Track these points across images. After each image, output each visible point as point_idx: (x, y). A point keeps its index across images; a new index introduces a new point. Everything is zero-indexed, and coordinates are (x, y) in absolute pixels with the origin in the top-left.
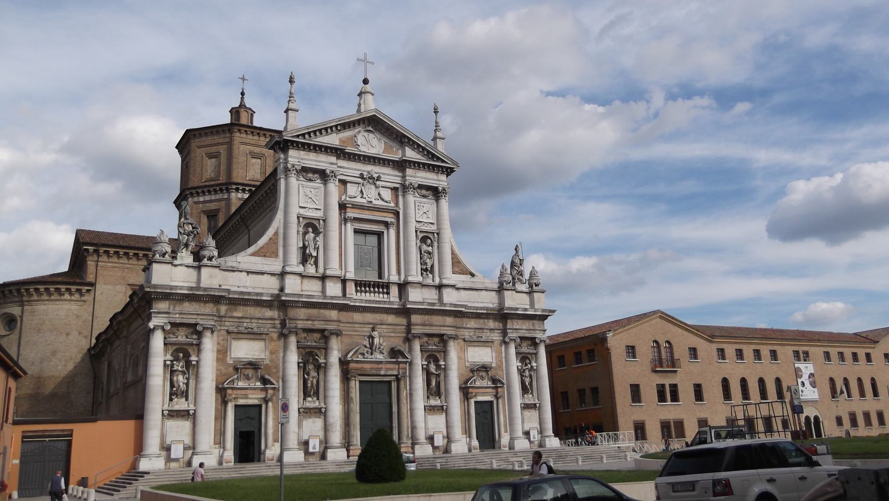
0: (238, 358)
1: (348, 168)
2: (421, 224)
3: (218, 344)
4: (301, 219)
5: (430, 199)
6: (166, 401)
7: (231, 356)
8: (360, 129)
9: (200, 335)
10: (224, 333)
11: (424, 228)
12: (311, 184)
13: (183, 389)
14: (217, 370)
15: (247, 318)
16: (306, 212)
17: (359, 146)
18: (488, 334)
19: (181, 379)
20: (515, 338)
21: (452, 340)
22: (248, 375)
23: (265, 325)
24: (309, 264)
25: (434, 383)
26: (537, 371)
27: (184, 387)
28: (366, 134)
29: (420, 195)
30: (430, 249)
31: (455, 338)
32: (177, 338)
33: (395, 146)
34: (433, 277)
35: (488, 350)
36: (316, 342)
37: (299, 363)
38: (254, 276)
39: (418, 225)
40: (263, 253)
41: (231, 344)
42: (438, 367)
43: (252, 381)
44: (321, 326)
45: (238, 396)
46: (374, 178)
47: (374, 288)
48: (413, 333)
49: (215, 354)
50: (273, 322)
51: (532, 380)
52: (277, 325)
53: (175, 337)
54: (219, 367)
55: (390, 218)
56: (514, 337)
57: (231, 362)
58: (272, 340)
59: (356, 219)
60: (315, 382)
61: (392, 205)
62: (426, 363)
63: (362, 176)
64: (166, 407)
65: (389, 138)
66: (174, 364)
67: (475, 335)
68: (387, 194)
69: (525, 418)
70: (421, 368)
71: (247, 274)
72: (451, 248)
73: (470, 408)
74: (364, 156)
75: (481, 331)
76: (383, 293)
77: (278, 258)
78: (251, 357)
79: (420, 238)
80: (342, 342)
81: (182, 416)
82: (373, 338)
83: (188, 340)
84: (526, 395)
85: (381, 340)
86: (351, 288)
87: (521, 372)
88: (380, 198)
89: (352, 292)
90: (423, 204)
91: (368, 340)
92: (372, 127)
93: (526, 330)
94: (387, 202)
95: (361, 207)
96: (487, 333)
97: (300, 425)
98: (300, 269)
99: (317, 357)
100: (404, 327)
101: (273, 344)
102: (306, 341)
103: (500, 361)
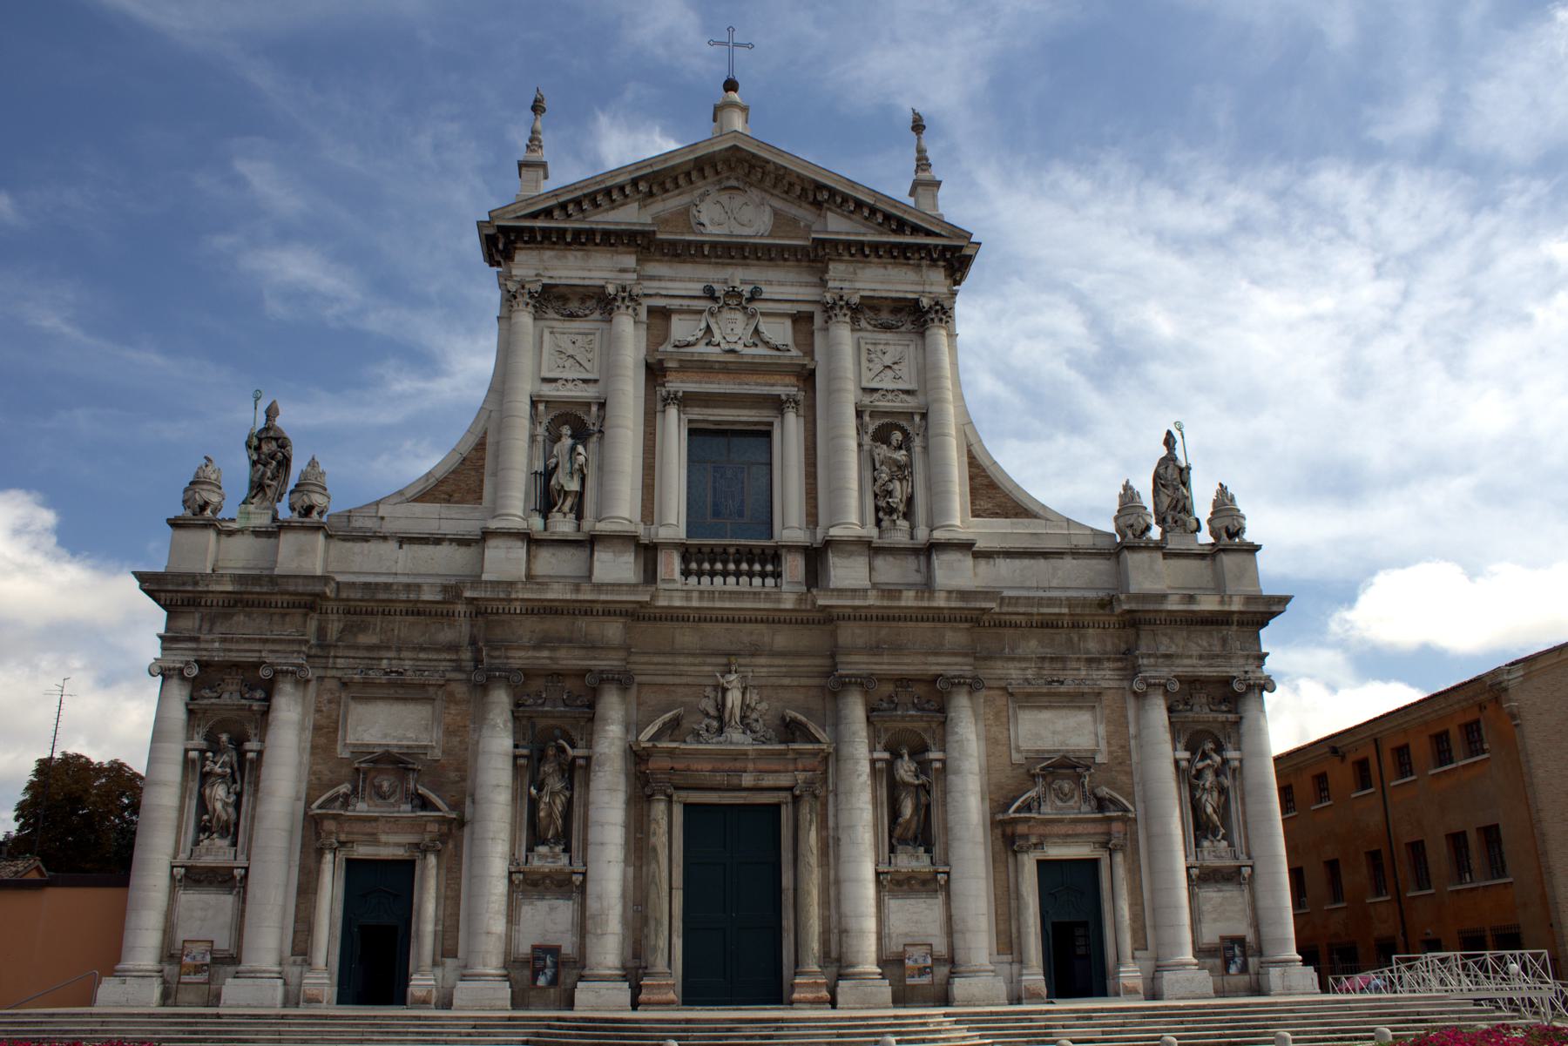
0: (362, 745)
1: (672, 280)
2: (876, 396)
3: (318, 711)
4: (541, 407)
5: (901, 332)
6: (185, 846)
7: (345, 740)
8: (708, 188)
9: (269, 690)
10: (331, 684)
11: (884, 404)
12: (577, 325)
13: (224, 817)
14: (309, 774)
15: (388, 648)
16: (558, 390)
20: (1162, 681)
21: (965, 689)
22: (381, 786)
23: (432, 664)
24: (560, 510)
25: (907, 809)
27: (226, 811)
28: (724, 198)
29: (875, 326)
30: (901, 456)
31: (974, 686)
32: (219, 697)
33: (804, 213)
34: (912, 527)
35: (1085, 717)
36: (566, 705)
37: (515, 757)
38: (416, 547)
39: (867, 400)
40: (445, 493)
42: (923, 767)
43: (392, 800)
44: (574, 662)
45: (355, 837)
46: (740, 295)
47: (738, 563)
48: (841, 676)
49: (308, 735)
50: (454, 657)
51: (1227, 801)
52: (464, 664)
53: (215, 695)
54: (315, 768)
55: (784, 388)
56: (1159, 678)
57: (346, 755)
58: (451, 699)
59: (685, 401)
61: (794, 352)
62: (886, 755)
63: (710, 294)
64: (183, 857)
66: (207, 759)
67: (1040, 676)
68: (779, 332)
70: (865, 768)
71: (397, 545)
72: (969, 452)
73: (1020, 879)
75: (1059, 665)
76: (763, 575)
77: (481, 504)
78: (395, 742)
79: (871, 429)
80: (639, 704)
81: (220, 882)
82: (725, 690)
83: (243, 702)
85: (753, 698)
86: (671, 565)
87: (1189, 778)
88: (762, 340)
89: (673, 575)
90: (881, 347)
91: (712, 695)
92: (737, 179)
94: (778, 349)
95: (705, 367)
96: (1079, 669)
97: (512, 917)
99: (561, 741)
100: (818, 661)
101: (453, 710)
102: (540, 701)
103: (1123, 747)
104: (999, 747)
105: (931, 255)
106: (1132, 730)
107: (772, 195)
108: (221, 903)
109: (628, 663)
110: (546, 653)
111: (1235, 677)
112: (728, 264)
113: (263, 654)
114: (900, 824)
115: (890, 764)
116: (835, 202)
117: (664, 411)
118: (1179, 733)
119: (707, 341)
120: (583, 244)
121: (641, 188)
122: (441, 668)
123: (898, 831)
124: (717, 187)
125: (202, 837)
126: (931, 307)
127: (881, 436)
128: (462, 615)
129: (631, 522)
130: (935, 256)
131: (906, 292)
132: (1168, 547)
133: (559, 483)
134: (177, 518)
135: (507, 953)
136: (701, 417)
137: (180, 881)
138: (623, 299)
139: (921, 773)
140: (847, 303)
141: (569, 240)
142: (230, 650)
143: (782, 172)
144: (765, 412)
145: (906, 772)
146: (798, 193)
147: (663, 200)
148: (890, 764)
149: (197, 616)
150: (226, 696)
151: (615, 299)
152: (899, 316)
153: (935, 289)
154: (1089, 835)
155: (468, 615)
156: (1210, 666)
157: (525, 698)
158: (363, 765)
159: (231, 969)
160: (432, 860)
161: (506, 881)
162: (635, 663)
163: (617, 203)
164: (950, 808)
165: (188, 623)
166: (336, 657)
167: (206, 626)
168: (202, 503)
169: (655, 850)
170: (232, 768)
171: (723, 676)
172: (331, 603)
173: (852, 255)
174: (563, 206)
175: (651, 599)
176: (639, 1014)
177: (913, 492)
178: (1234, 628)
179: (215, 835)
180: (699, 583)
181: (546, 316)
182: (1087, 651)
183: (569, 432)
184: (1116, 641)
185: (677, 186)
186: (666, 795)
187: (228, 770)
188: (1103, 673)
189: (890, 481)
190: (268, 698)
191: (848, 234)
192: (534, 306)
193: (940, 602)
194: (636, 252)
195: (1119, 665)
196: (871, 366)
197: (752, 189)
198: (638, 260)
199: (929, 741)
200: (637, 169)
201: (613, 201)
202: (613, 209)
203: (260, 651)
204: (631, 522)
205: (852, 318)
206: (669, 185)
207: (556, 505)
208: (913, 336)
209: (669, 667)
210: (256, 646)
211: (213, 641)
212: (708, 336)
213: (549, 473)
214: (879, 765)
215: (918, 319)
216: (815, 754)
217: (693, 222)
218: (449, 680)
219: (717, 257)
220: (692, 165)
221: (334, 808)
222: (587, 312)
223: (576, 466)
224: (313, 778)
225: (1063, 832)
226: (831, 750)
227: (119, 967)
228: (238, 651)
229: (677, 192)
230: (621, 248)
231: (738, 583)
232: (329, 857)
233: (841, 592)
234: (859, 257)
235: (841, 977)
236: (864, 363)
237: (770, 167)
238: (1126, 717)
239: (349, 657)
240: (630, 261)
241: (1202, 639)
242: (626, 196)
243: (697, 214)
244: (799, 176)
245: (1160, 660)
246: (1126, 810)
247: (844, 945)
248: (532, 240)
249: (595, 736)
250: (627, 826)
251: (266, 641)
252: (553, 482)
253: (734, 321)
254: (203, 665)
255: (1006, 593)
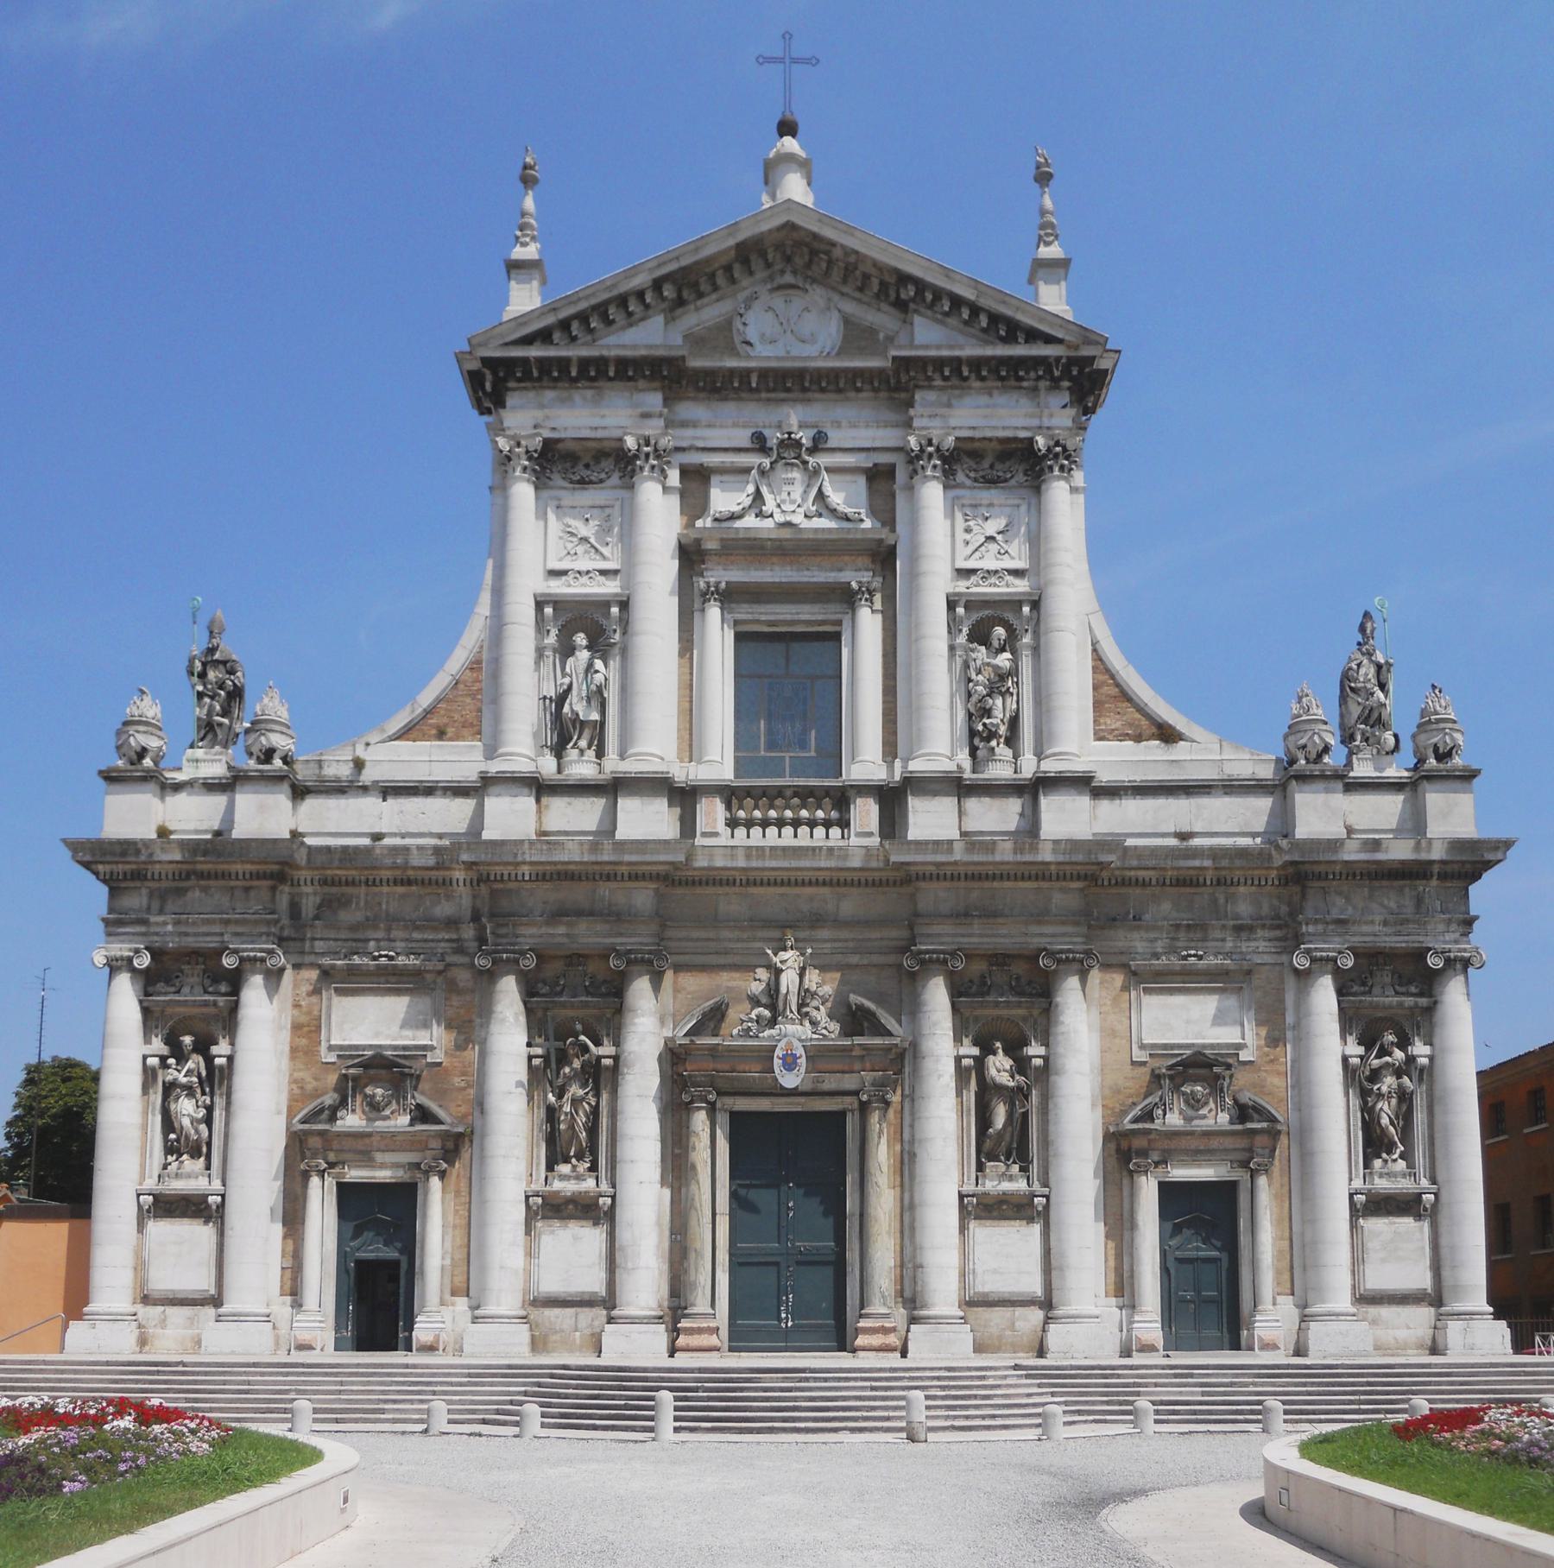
2: (974, 579)
3: (297, 1006)
5: (1010, 488)
6: (151, 1170)
9: (235, 982)
14: (290, 1083)
16: (569, 586)
17: (749, 343)
18: (1229, 945)
19: (187, 1109)
26: (1427, 1075)
27: (197, 1131)
28: (778, 301)
29: (976, 480)
33: (882, 319)
34: (1016, 756)
36: (588, 994)
37: (530, 1058)
41: (329, 1007)
43: (387, 1112)
46: (798, 444)
48: (920, 952)
49: (286, 1036)
50: (454, 936)
52: (466, 944)
53: (173, 989)
54: (296, 1075)
57: (332, 1058)
58: (453, 988)
60: (581, 1119)
61: (868, 524)
62: (976, 1051)
64: (150, 1183)
65: (859, 301)
69: (1372, 1245)
72: (1095, 650)
74: (764, 374)
75: (1199, 935)
76: (827, 824)
80: (676, 991)
83: (207, 998)
84: (1377, 1163)
86: (712, 813)
87: (1360, 1081)
92: (795, 272)
93: (1385, 923)
94: (848, 519)
96: (1223, 940)
98: (547, 766)
99: (582, 1038)
100: (894, 933)
101: (456, 1001)
104: (1117, 1041)
105: (1051, 372)
106: (1290, 1019)
107: (842, 294)
108: (200, 1234)
109: (663, 939)
110: (561, 930)
111: (1430, 949)
112: (783, 400)
113: (226, 938)
114: (990, 1137)
115: (980, 1062)
116: (924, 300)
117: (703, 610)
118: (1351, 1023)
119: (757, 511)
120: (593, 379)
121: (666, 294)
122: (440, 951)
123: (988, 1144)
124: (769, 286)
125: (170, 1159)
126: (1049, 450)
127: (980, 635)
128: (461, 883)
129: (662, 759)
130: (1057, 373)
131: (1017, 428)
132: (1351, 774)
133: (572, 710)
134: (109, 770)
135: (526, 1291)
136: (750, 617)
137: (149, 1211)
138: (647, 455)
139: (1020, 1074)
140: (938, 449)
141: (574, 373)
142: (187, 934)
143: (852, 259)
144: (832, 607)
145: (999, 1071)
146: (876, 288)
147: (697, 309)
148: (980, 1062)
149: (144, 891)
150: (186, 990)
151: (636, 457)
152: (1008, 464)
153: (1055, 422)
154: (1226, 1150)
155: (468, 883)
156: (1398, 934)
157: (540, 985)
158: (351, 1071)
159: (210, 1311)
160: (435, 1182)
161: (523, 1207)
162: (670, 939)
163: (637, 317)
164: (1051, 1117)
165: (135, 901)
166: (313, 939)
167: (156, 905)
168: (139, 749)
169: (694, 1167)
170: (199, 1076)
171: (776, 955)
172: (304, 872)
173: (945, 379)
174: (565, 325)
175: (687, 859)
176: (681, 1360)
177: (1018, 709)
178: (1434, 882)
179: (185, 1157)
180: (748, 837)
181: (551, 483)
182: (1237, 917)
183: (585, 642)
184: (1275, 902)
185: (716, 288)
186: (708, 1102)
187: (195, 1080)
188: (1253, 944)
189: (989, 695)
190: (235, 991)
191: (938, 347)
192: (534, 470)
193: (1046, 855)
194: (663, 388)
195: (1278, 933)
196: (968, 537)
197: (815, 286)
198: (667, 401)
199: (1029, 1033)
200: (659, 266)
201: (630, 314)
202: (631, 325)
203: (222, 934)
204: (662, 759)
205: (944, 471)
206: (704, 287)
207: (571, 739)
208: (1024, 492)
209: (712, 944)
210: (217, 929)
211: (165, 924)
212: (758, 502)
213: (562, 698)
214: (966, 1062)
215: (1032, 468)
216: (888, 1049)
217: (737, 340)
218: (449, 965)
219: (769, 391)
220: (733, 253)
221: (320, 1122)
222: (603, 476)
223: (593, 687)
224: (294, 1086)
225: (1193, 1147)
226: (906, 1045)
227: (86, 1309)
228: (196, 935)
229: (714, 296)
230: (641, 384)
231: (796, 836)
232: (315, 1181)
233: (920, 845)
234: (955, 381)
235: (913, 1320)
236: (961, 535)
237: (837, 253)
238: (1282, 1001)
239: (329, 939)
240: (654, 400)
241: (1389, 899)
242: (647, 307)
243: (741, 327)
244: (875, 264)
245: (1331, 927)
246: (1273, 1120)
247: (920, 1283)
248: (527, 376)
249: (623, 1031)
250: (663, 1141)
251: (227, 922)
252: (566, 709)
253: (791, 482)
254: (156, 954)
255: (1130, 842)
